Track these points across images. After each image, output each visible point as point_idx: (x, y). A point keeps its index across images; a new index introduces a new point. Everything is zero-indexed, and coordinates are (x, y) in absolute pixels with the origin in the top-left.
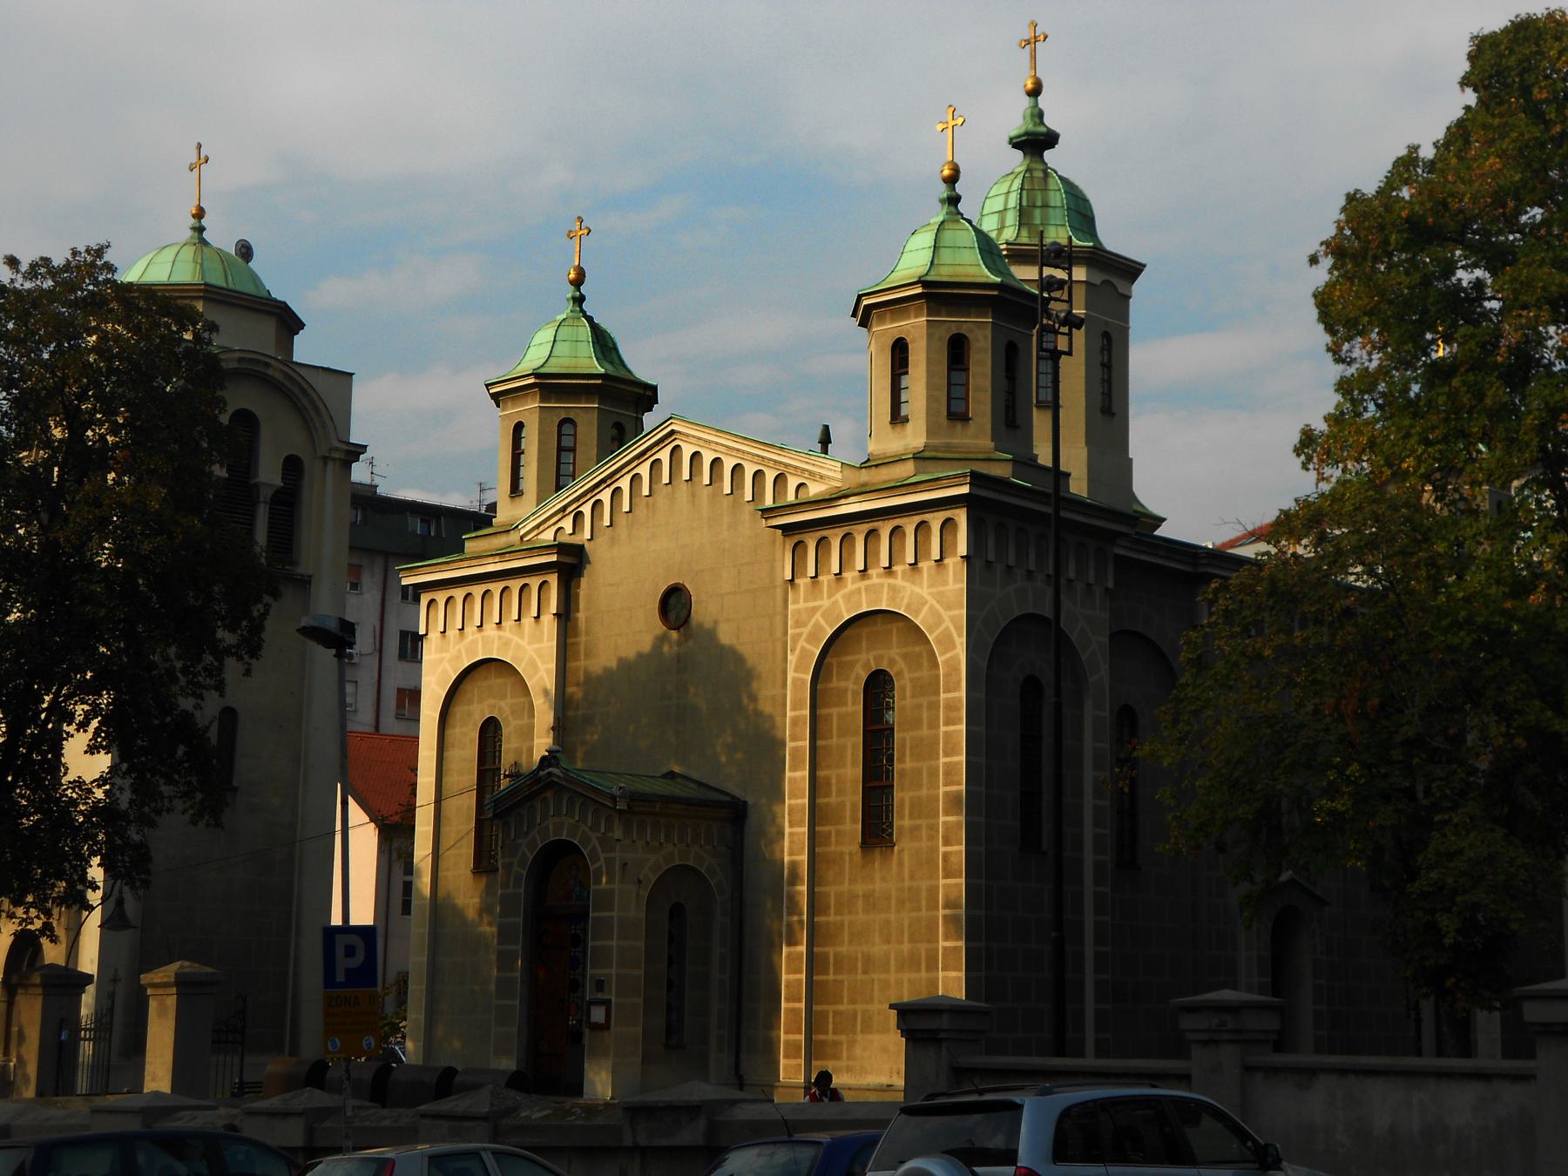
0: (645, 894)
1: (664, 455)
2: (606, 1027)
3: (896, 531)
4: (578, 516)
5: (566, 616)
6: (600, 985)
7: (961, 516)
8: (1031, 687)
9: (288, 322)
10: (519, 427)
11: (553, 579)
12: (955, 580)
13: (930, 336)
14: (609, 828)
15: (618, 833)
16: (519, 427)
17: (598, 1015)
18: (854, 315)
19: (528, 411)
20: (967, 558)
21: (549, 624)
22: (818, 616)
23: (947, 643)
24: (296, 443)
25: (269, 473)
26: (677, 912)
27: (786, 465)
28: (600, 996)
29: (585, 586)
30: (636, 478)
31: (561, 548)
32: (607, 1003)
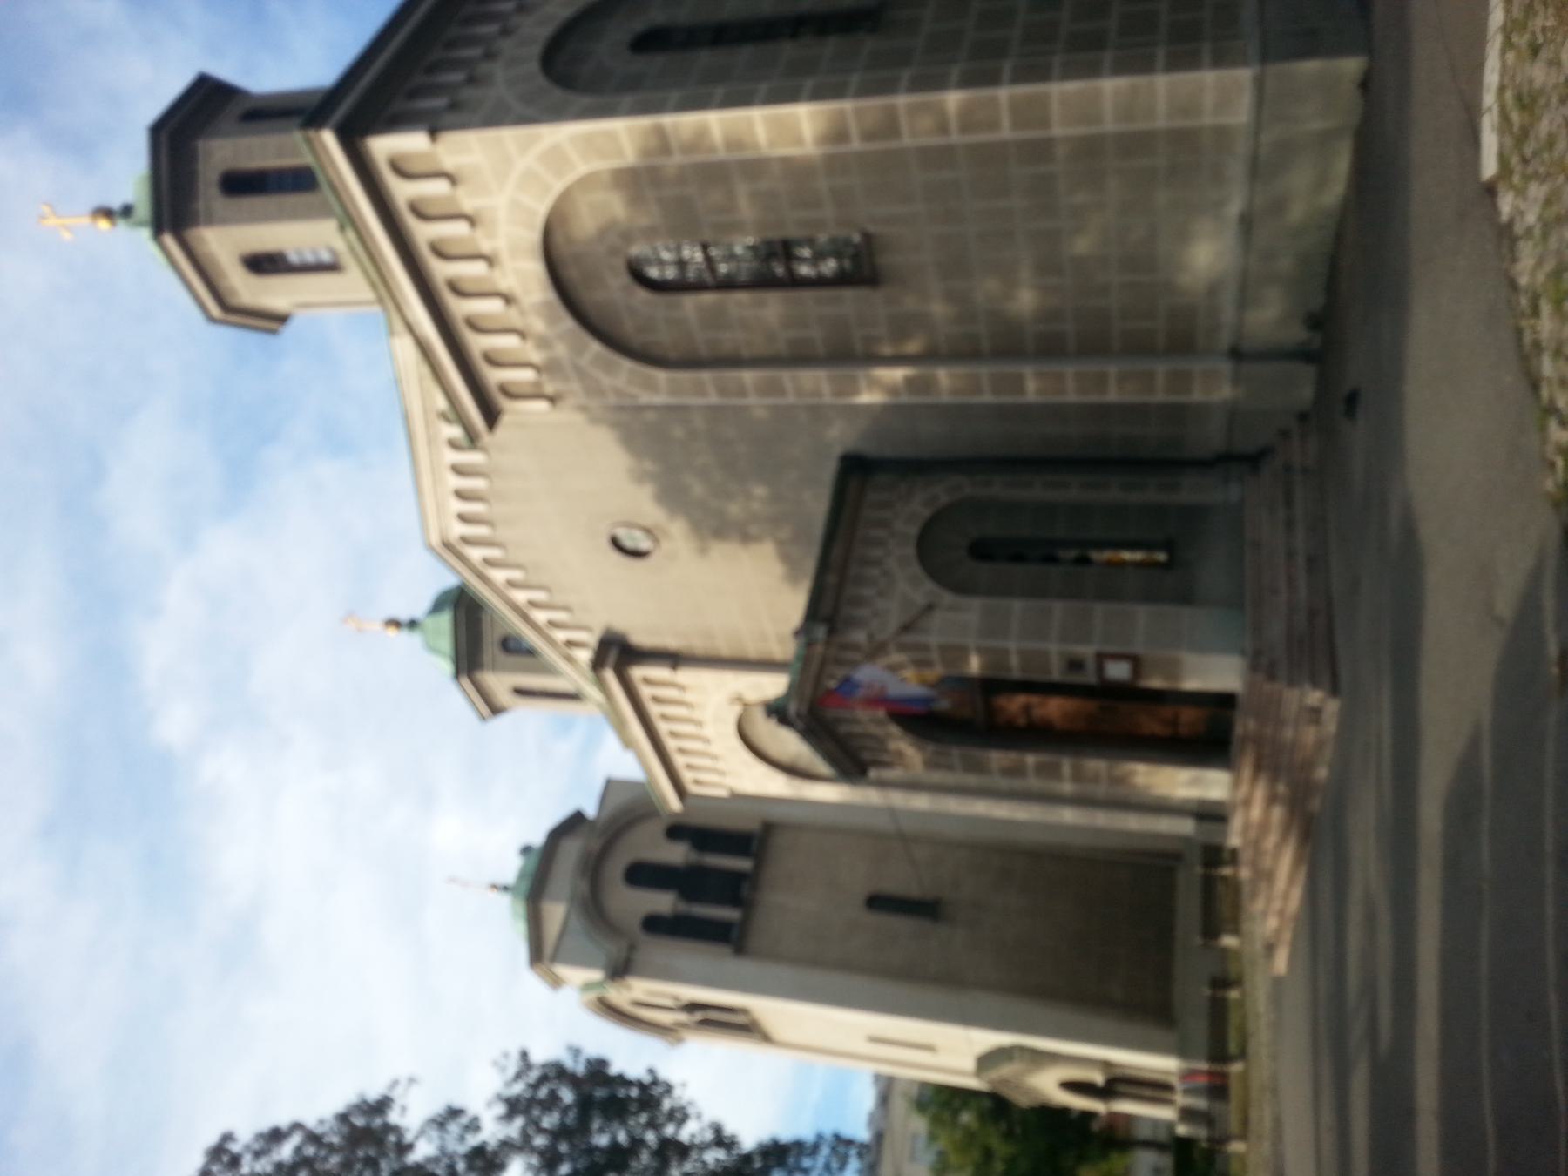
0: (948, 598)
1: (476, 554)
2: (1135, 661)
3: (439, 252)
4: (570, 644)
5: (674, 659)
6: (1075, 665)
7: (382, 146)
8: (648, 42)
9: (575, 822)
10: (521, 692)
11: (638, 673)
12: (465, 149)
13: (224, 221)
14: (855, 647)
15: (859, 636)
16: (521, 692)
17: (1118, 671)
18: (273, 332)
19: (499, 682)
20: (434, 132)
21: (685, 676)
22: (584, 361)
23: (555, 158)
24: (655, 829)
25: (677, 854)
26: (981, 551)
27: (425, 412)
28: (1091, 665)
29: (641, 638)
30: (511, 584)
31: (598, 664)
32: (1101, 658)
